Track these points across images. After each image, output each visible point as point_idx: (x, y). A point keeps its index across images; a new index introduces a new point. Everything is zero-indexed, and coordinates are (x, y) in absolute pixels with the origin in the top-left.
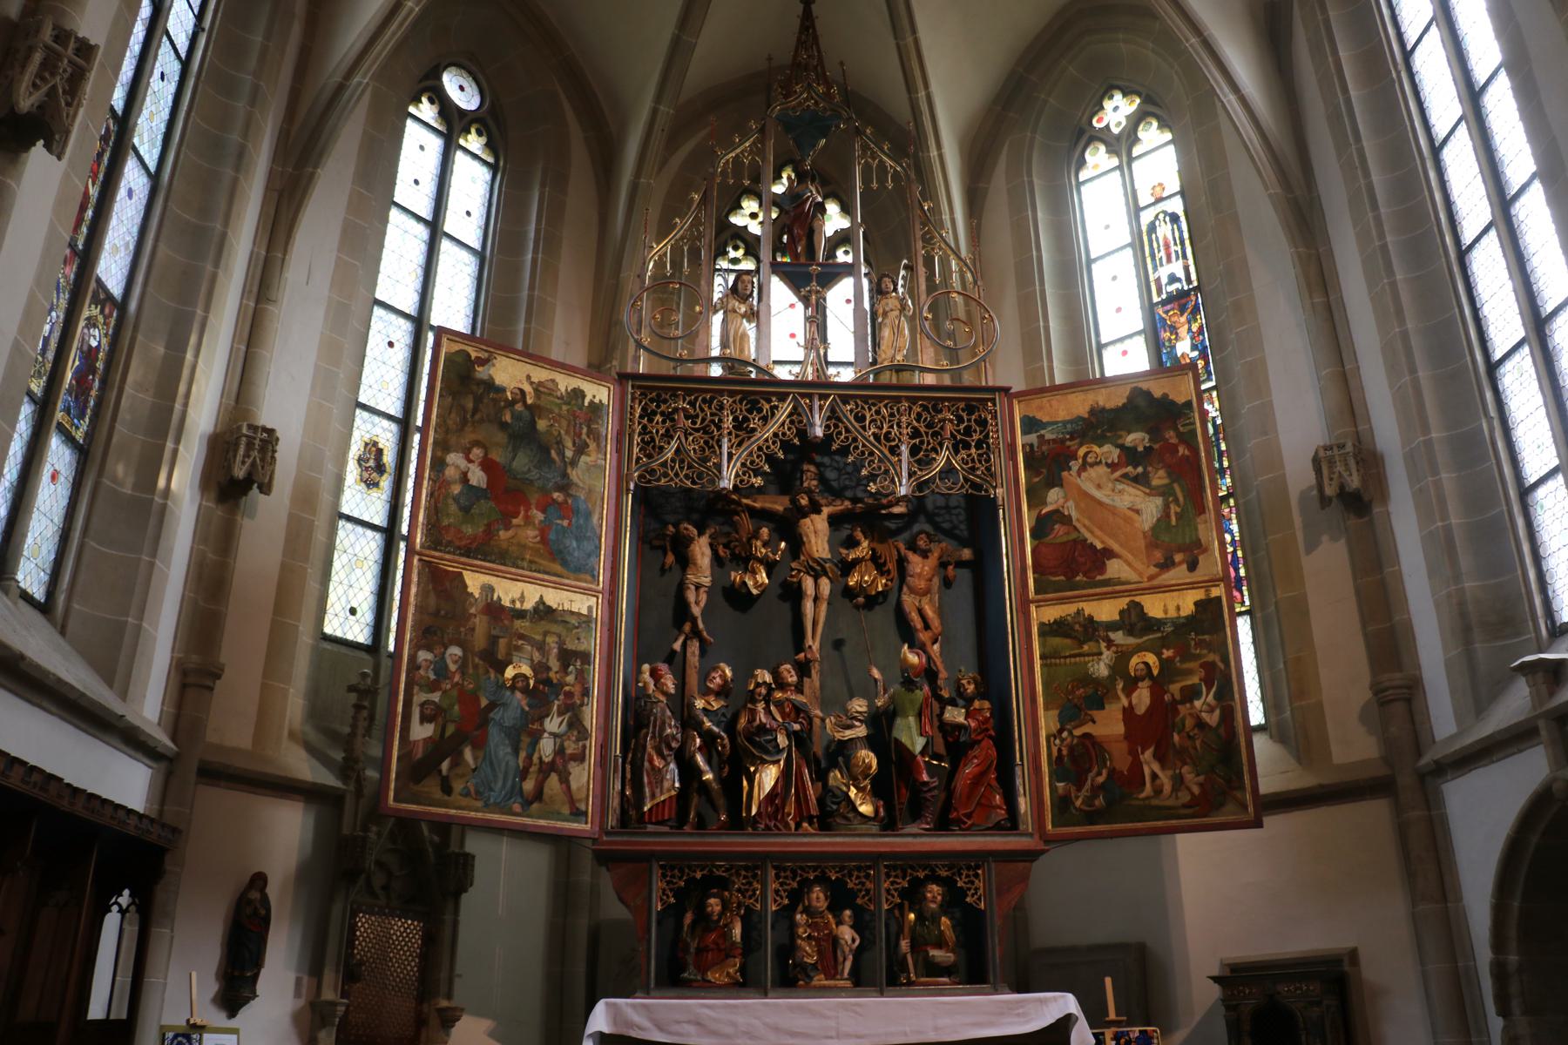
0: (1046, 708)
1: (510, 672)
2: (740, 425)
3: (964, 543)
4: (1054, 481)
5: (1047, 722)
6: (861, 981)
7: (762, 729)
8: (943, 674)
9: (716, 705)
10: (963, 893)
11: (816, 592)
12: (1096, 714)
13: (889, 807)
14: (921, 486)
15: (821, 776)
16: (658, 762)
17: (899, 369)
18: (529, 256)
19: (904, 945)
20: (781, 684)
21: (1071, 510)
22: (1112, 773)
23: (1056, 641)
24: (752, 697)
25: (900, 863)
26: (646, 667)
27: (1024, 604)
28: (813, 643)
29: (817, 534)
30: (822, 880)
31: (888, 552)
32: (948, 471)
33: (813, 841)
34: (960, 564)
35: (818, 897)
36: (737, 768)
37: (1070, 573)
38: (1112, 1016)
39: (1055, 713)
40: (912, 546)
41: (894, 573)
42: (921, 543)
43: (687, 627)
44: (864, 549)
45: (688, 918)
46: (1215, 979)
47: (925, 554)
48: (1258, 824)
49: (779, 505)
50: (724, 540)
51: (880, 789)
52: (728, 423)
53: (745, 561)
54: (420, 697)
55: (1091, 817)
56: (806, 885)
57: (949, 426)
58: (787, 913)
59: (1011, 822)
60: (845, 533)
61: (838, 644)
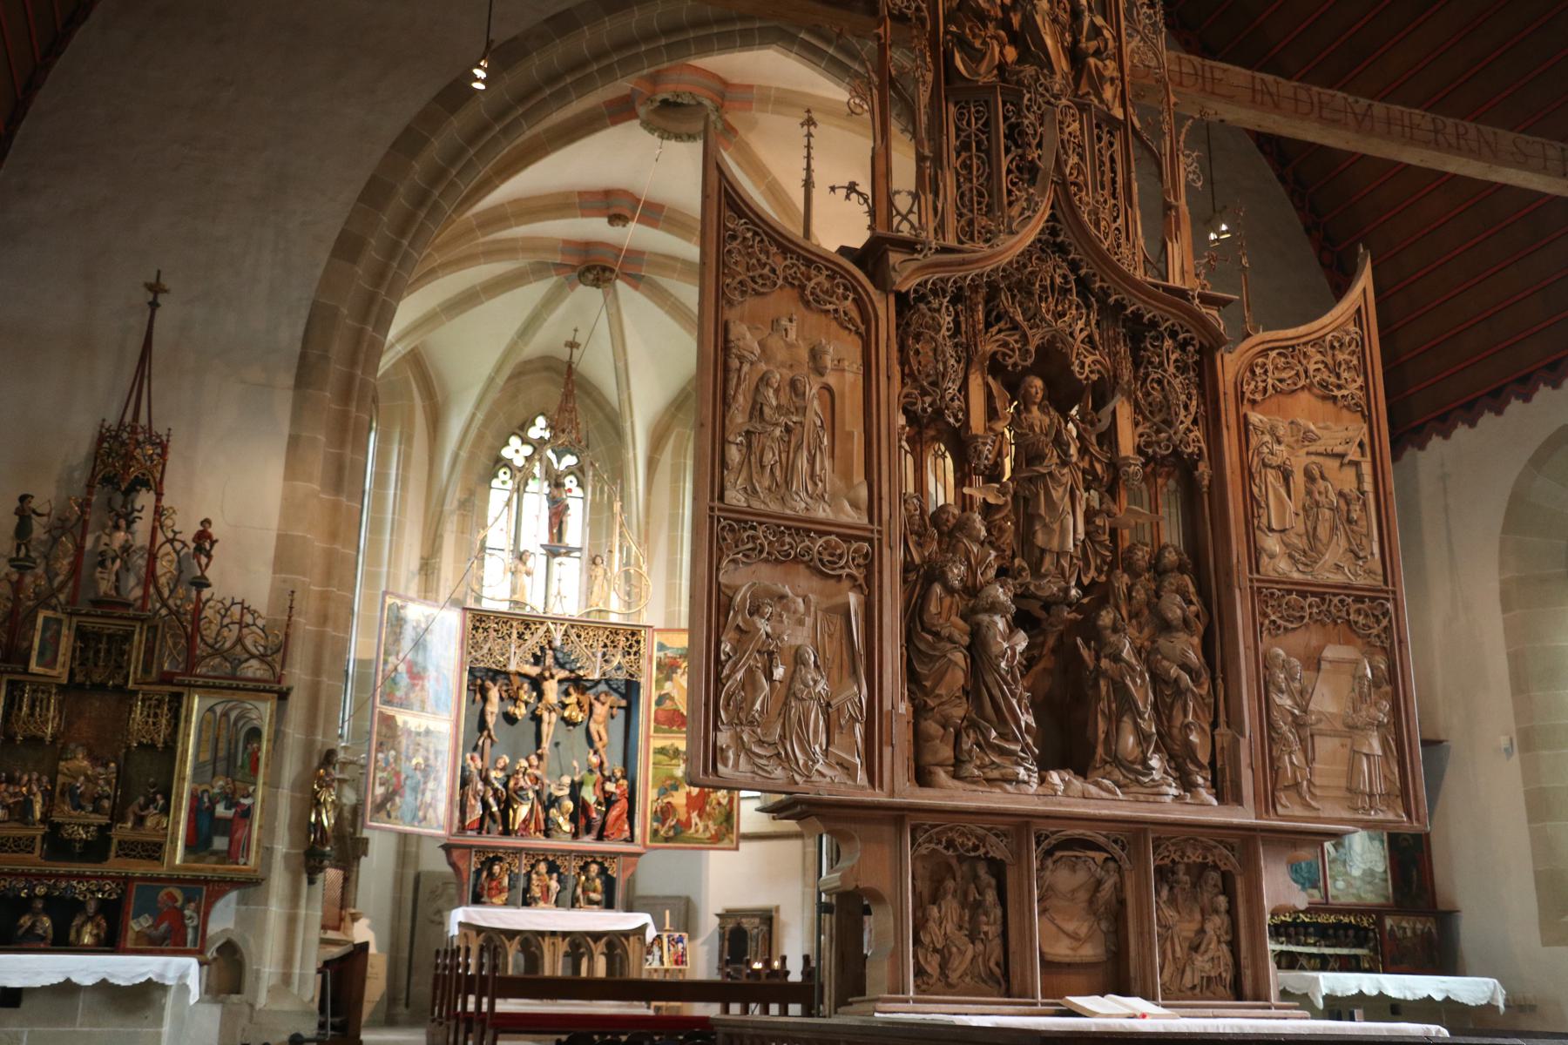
0: (653, 787)
1: (414, 762)
2: (520, 636)
3: (623, 696)
4: (669, 678)
5: (653, 794)
6: (557, 903)
7: (522, 788)
8: (606, 765)
9: (500, 775)
10: (607, 869)
11: (550, 720)
12: (674, 793)
13: (576, 827)
14: (604, 674)
15: (546, 809)
16: (473, 802)
17: (600, 611)
18: (392, 492)
19: (579, 891)
20: (530, 766)
21: (675, 694)
22: (678, 821)
23: (661, 757)
24: (517, 772)
25: (580, 854)
26: (468, 756)
27: (648, 737)
28: (546, 744)
29: (552, 690)
30: (545, 860)
31: (585, 700)
32: (619, 668)
33: (540, 842)
34: (619, 707)
35: (542, 867)
36: (507, 804)
37: (671, 725)
38: (667, 927)
39: (656, 791)
40: (597, 699)
41: (587, 712)
42: (602, 698)
43: (486, 733)
44: (573, 699)
45: (485, 874)
46: (718, 915)
47: (603, 704)
48: (737, 849)
49: (534, 671)
50: (505, 688)
51: (573, 818)
52: (515, 635)
53: (515, 700)
54: (379, 775)
55: (667, 840)
56: (538, 861)
57: (622, 644)
58: (528, 874)
59: (631, 839)
60: (564, 686)
61: (557, 744)
